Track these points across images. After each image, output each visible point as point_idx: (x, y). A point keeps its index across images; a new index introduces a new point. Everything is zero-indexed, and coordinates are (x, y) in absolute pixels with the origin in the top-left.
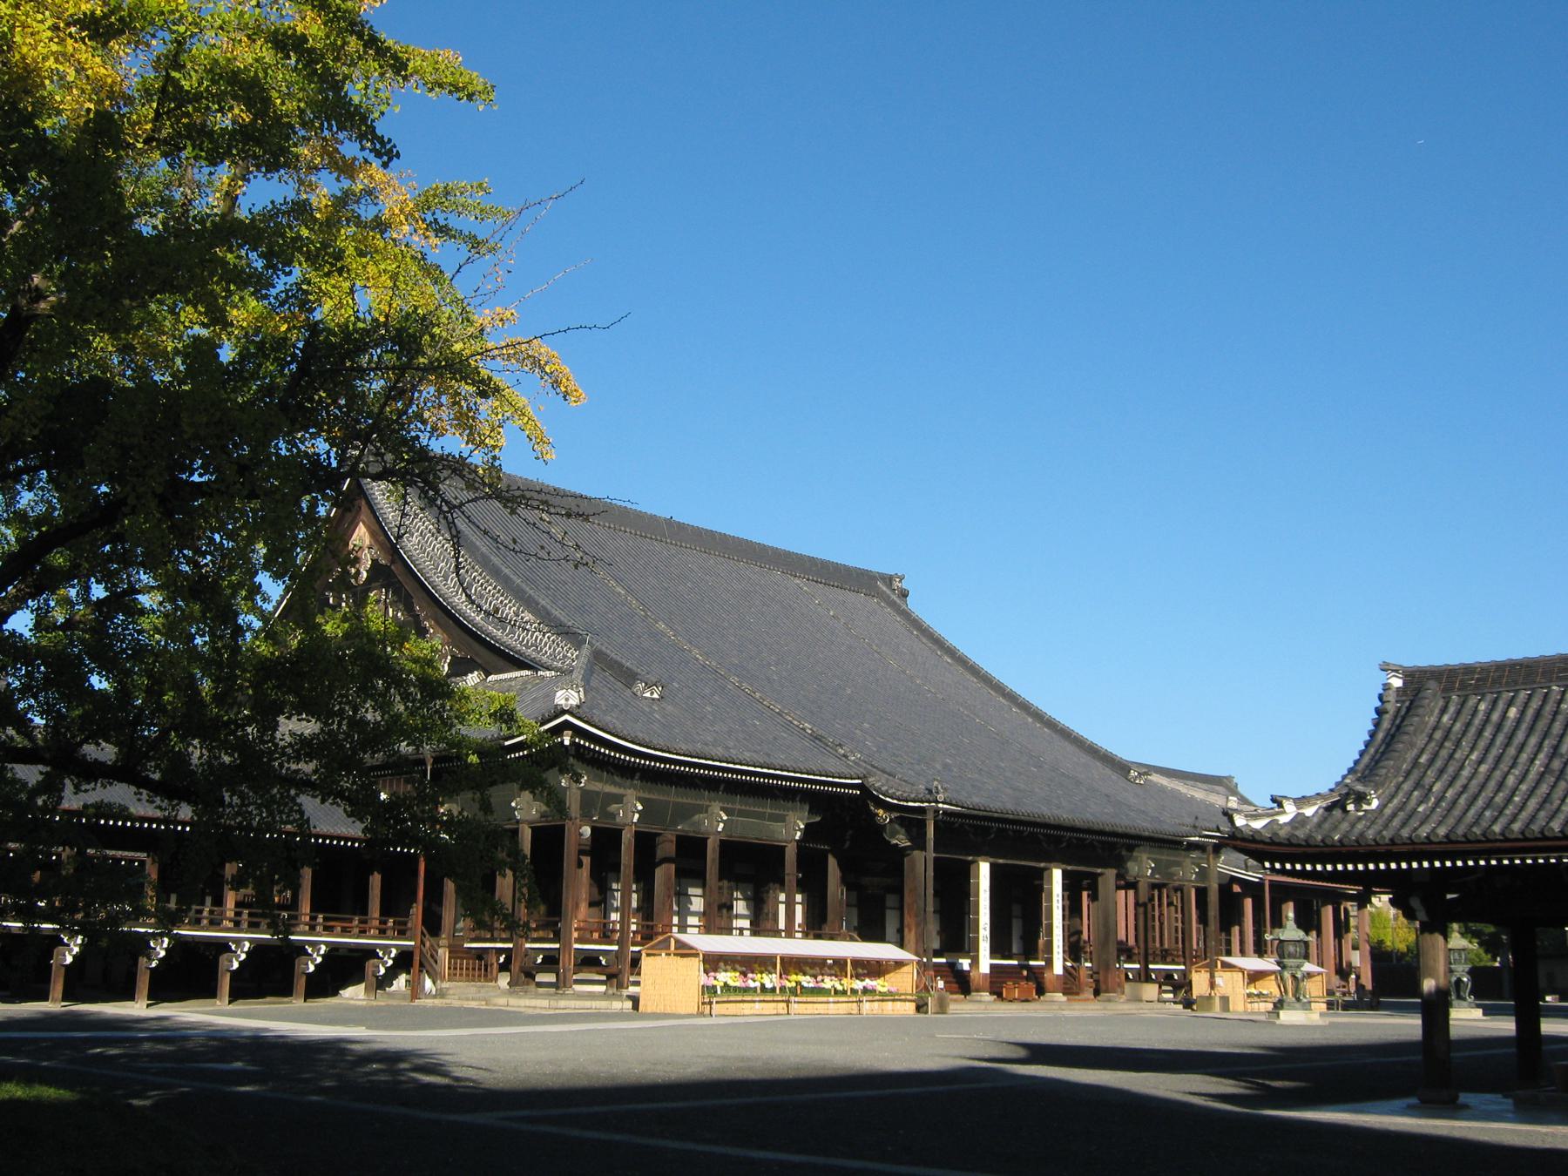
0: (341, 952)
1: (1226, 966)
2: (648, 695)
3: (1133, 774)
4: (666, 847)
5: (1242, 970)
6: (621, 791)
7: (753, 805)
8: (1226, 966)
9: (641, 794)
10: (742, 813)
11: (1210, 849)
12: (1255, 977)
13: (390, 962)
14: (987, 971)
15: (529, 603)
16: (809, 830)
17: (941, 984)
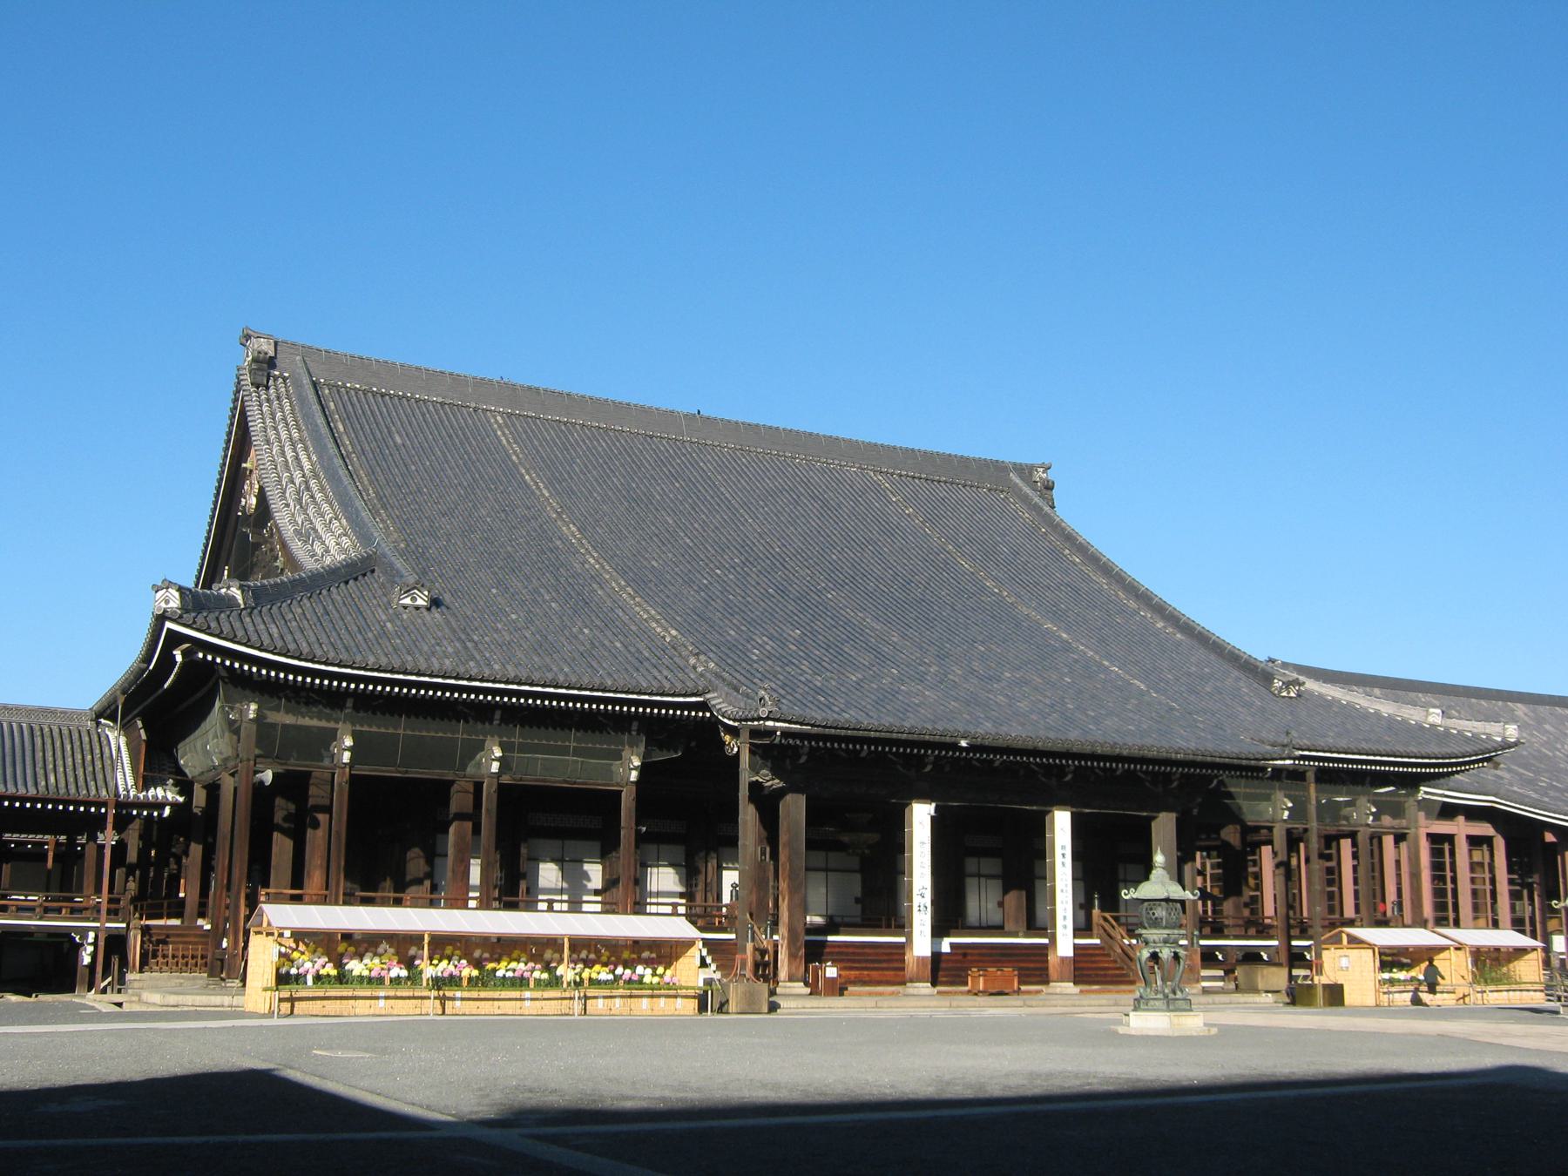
0: (36, 938)
1: (1355, 941)
2: (407, 601)
3: (1277, 684)
4: (459, 801)
5: (1371, 946)
6: (332, 725)
7: (540, 737)
8: (1355, 941)
9: (358, 728)
10: (523, 748)
11: (1311, 776)
12: (1391, 959)
13: (90, 949)
14: (928, 953)
15: (346, 505)
16: (643, 769)
17: (831, 972)
